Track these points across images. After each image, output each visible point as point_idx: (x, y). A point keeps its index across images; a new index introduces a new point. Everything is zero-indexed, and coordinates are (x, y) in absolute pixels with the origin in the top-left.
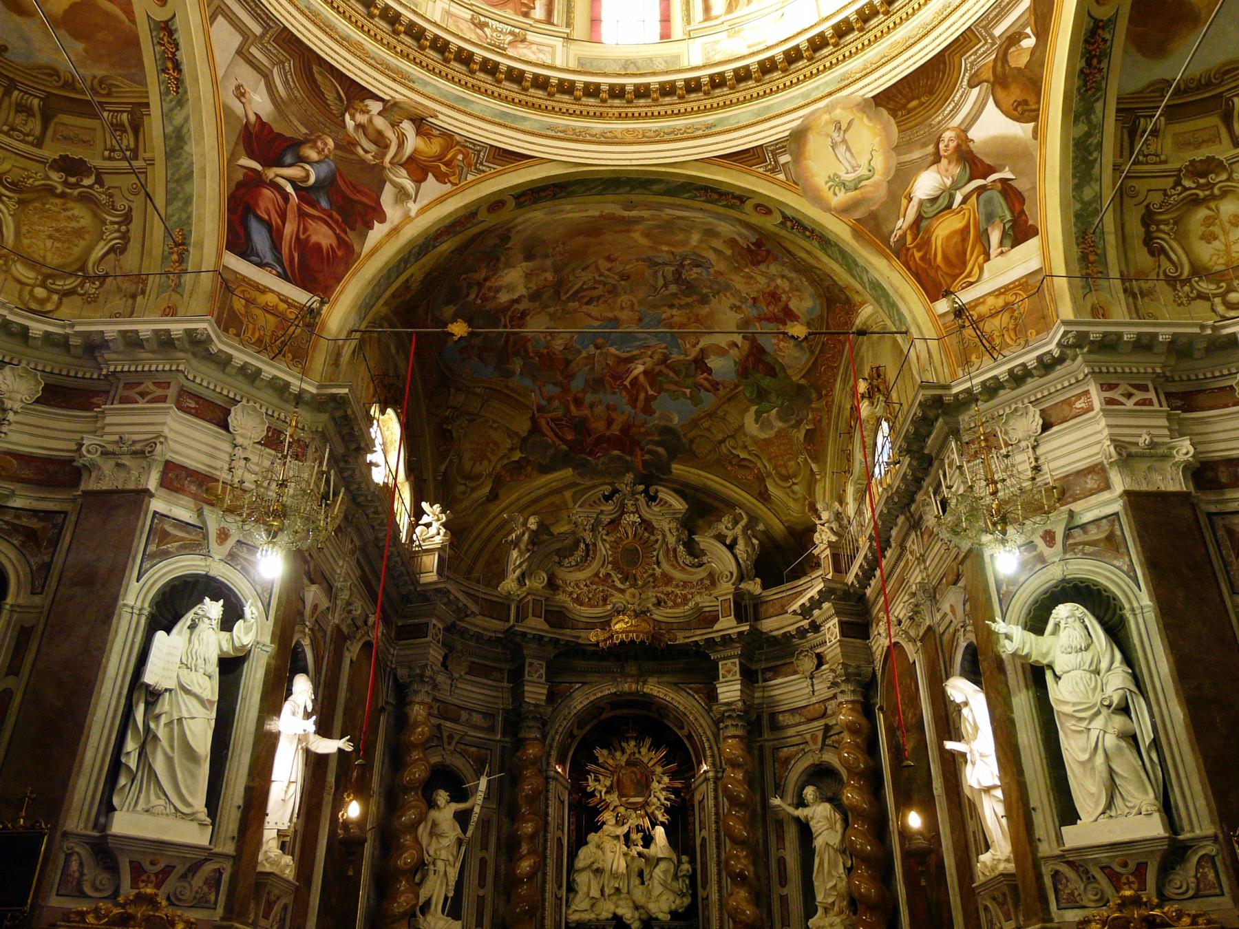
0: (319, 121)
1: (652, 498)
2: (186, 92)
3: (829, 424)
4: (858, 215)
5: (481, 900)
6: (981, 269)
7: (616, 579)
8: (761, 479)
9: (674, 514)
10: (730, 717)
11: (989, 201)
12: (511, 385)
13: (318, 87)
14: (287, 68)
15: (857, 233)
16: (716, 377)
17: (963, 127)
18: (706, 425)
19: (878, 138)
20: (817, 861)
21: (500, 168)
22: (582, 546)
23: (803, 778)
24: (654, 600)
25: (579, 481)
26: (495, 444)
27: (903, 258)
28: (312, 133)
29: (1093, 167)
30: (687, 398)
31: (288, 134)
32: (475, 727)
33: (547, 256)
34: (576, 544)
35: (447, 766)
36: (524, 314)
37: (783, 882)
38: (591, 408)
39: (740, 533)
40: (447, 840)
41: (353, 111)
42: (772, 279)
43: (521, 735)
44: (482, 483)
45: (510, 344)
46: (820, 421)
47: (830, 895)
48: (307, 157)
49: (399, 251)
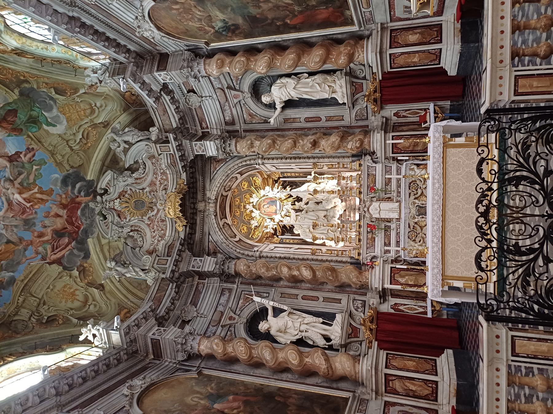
1: (106, 191)
5: (326, 300)
7: (152, 214)
8: (95, 126)
9: (114, 179)
10: (225, 149)
12: (22, 278)
16: (23, 149)
18: (60, 157)
20: (305, 96)
22: (131, 234)
23: (260, 105)
24: (164, 192)
25: (95, 235)
26: (65, 286)
30: (40, 169)
32: (228, 301)
34: (132, 237)
35: (247, 320)
37: (319, 119)
38: (45, 227)
39: (121, 139)
40: (289, 322)
43: (233, 273)
44: (91, 294)
46: (46, 84)
47: (324, 89)
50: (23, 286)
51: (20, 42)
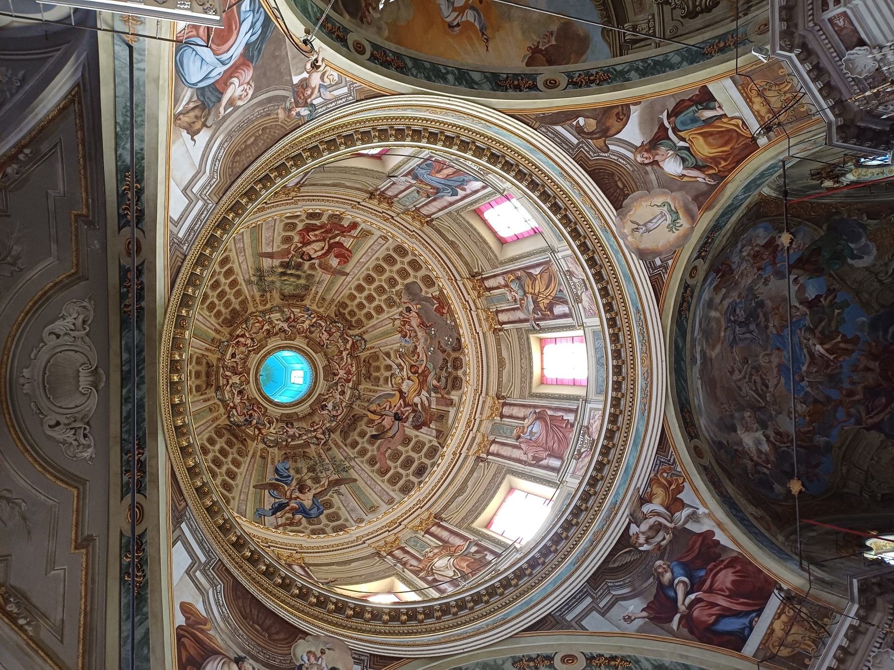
0: (645, 568)
2: (630, 656)
3: (862, 203)
4: (695, 209)
6: (733, 118)
11: (683, 123)
13: (623, 565)
14: (612, 584)
15: (709, 208)
17: (634, 150)
18: (866, 296)
19: (643, 203)
21: (671, 449)
27: (726, 174)
28: (653, 574)
29: (658, 61)
31: (654, 591)
33: (732, 416)
36: (778, 433)
41: (637, 544)
42: (743, 259)
45: (804, 444)
46: (859, 210)
48: (670, 580)
49: (735, 524)
50: (842, 454)
51: (856, 175)
